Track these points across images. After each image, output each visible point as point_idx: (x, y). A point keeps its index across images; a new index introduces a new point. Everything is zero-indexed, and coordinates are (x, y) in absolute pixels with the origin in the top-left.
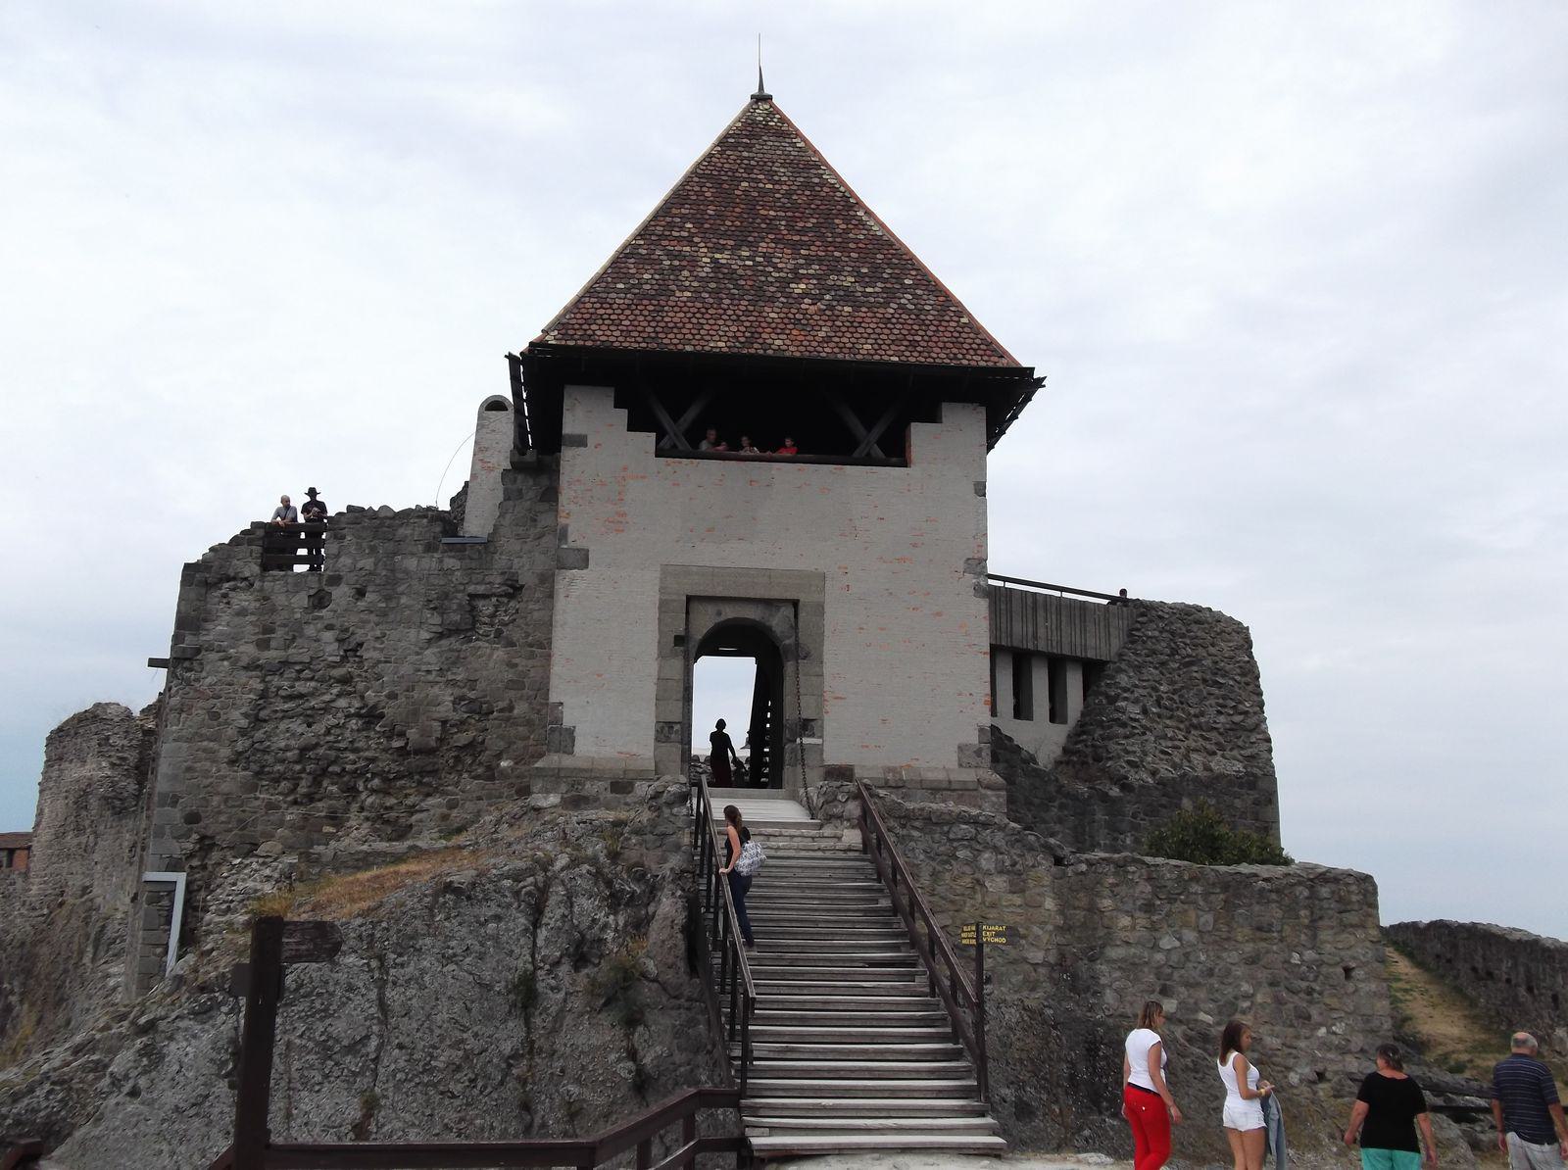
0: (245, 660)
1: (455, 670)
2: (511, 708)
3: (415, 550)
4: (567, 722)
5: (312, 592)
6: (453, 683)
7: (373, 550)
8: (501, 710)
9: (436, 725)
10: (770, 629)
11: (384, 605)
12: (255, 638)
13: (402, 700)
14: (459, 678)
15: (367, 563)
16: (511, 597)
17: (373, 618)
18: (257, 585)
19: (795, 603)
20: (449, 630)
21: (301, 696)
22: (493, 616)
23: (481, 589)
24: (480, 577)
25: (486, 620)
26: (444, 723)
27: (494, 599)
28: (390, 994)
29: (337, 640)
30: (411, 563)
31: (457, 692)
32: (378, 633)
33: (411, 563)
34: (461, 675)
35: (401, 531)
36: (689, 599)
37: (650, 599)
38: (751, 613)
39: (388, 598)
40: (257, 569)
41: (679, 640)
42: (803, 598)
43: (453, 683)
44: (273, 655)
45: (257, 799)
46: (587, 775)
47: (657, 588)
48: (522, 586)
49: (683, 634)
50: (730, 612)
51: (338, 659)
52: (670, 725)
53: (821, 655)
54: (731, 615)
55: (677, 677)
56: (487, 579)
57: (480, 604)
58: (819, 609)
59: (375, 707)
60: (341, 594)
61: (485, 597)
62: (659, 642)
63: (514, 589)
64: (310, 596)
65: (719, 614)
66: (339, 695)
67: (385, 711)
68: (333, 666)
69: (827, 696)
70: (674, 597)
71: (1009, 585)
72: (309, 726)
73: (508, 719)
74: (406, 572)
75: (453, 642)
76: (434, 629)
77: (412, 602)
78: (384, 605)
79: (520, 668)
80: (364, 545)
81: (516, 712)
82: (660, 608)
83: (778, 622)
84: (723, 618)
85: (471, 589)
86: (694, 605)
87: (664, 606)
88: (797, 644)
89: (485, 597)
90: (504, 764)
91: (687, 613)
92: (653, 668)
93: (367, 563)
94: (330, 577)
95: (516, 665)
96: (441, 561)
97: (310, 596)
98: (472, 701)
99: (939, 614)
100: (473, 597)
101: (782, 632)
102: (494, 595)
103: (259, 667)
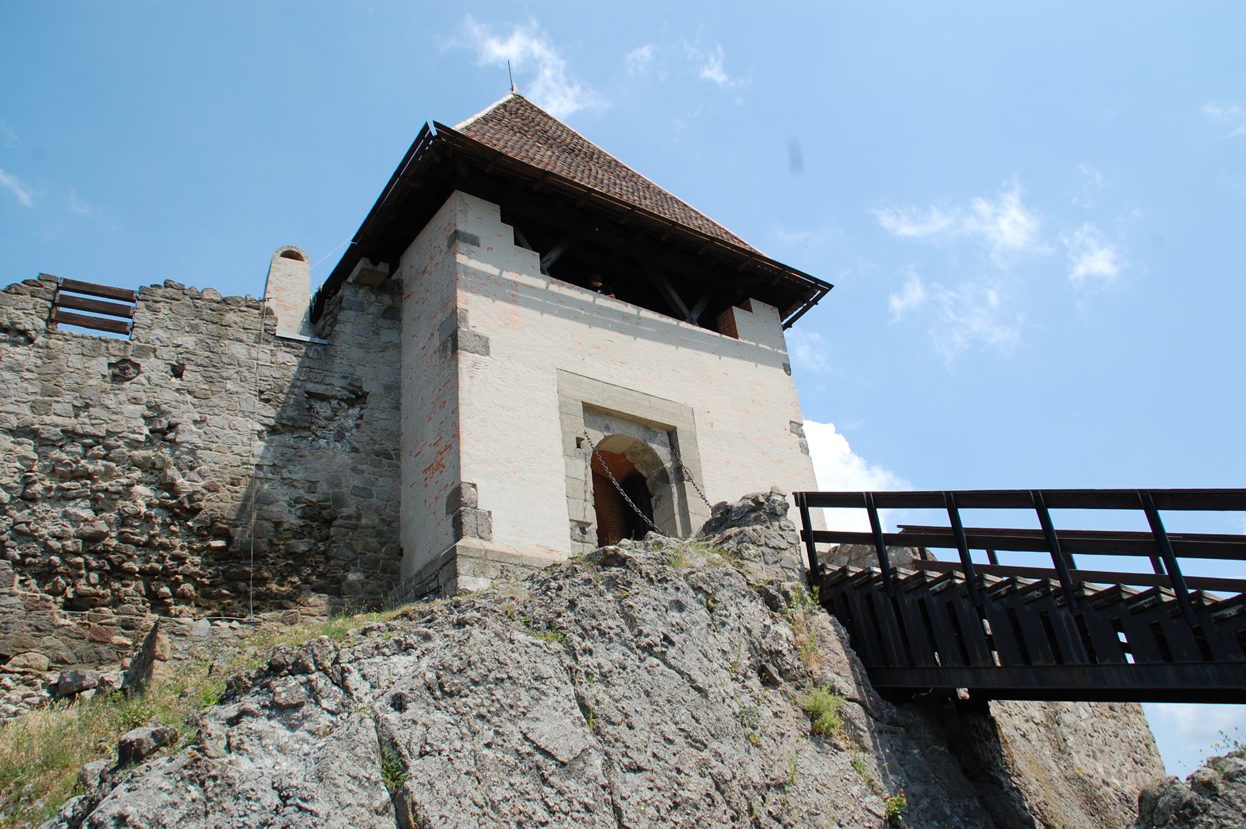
0: (14, 422)
1: (292, 468)
2: (359, 517)
3: (244, 337)
4: (483, 506)
5: (113, 360)
6: (291, 483)
7: (194, 329)
8: (349, 517)
9: (268, 525)
11: (206, 387)
12: (32, 398)
13: (224, 493)
14: (295, 477)
15: (189, 341)
16: (351, 403)
17: (189, 398)
18: (40, 340)
20: (284, 425)
21: (89, 476)
22: (331, 419)
23: (320, 389)
24: (320, 378)
25: (323, 423)
26: (278, 524)
27: (334, 402)
28: (593, 691)
29: (145, 417)
30: (239, 351)
31: (296, 493)
32: (197, 417)
33: (239, 351)
34: (299, 474)
35: (231, 317)
37: (551, 400)
39: (209, 380)
40: (43, 324)
43: (291, 483)
44: (57, 419)
45: (11, 595)
46: (516, 562)
48: (365, 395)
50: (618, 429)
51: (142, 438)
54: (618, 432)
56: (327, 380)
57: (317, 405)
59: (190, 497)
60: (153, 367)
61: (323, 398)
63: (357, 397)
64: (110, 365)
66: (139, 482)
67: (202, 504)
68: (134, 445)
71: (677, 517)
72: (97, 512)
73: (355, 528)
74: (232, 357)
75: (288, 438)
76: (266, 421)
77: (240, 390)
78: (206, 387)
79: (366, 475)
80: (183, 322)
81: (363, 521)
82: (560, 407)
85: (310, 387)
88: (679, 469)
89: (323, 398)
90: (352, 577)
92: (560, 463)
93: (189, 341)
94: (140, 348)
95: (363, 472)
96: (273, 355)
97: (110, 365)
98: (310, 505)
99: (780, 461)
100: (311, 395)
102: (335, 397)
103: (33, 434)
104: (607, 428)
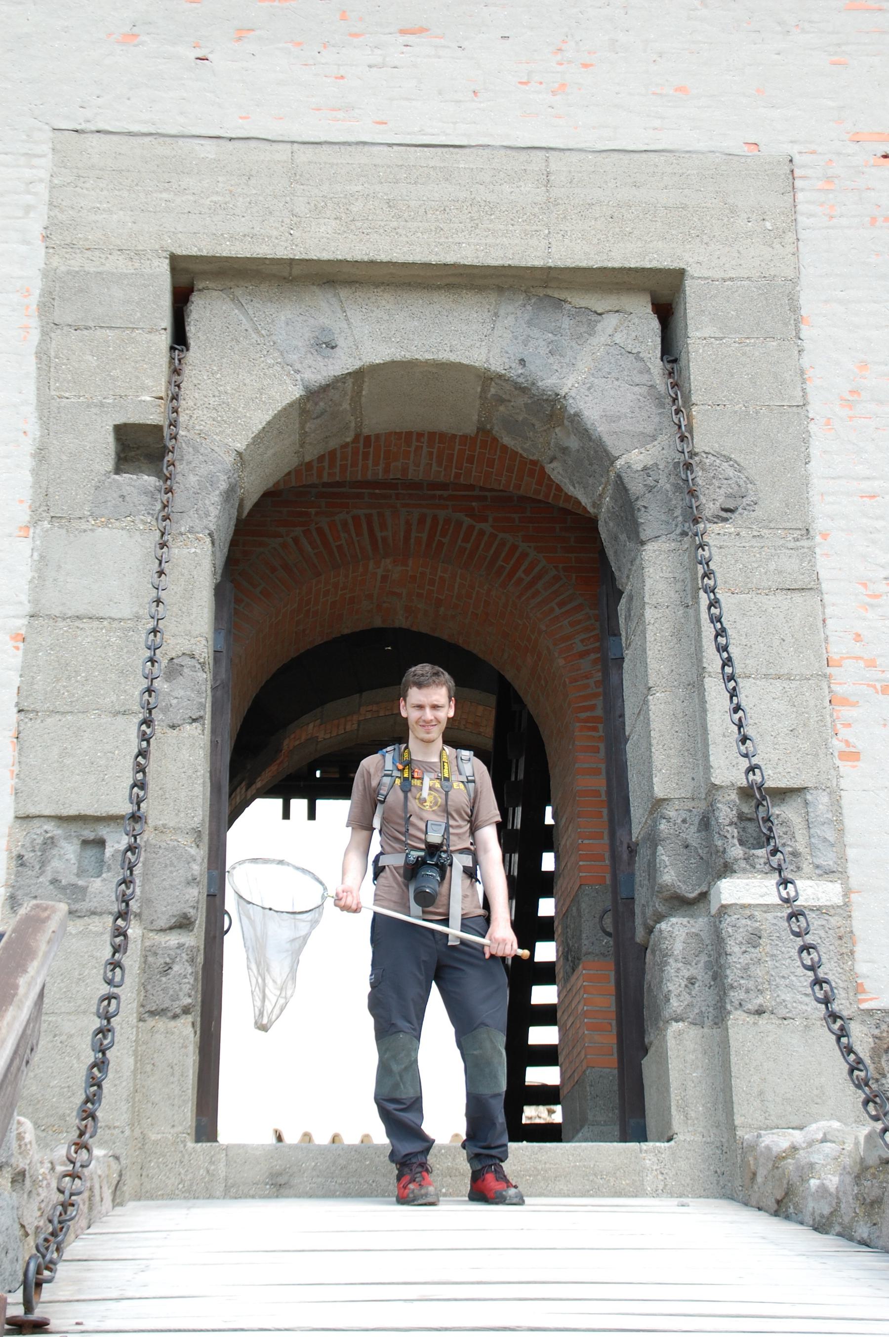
10: (551, 410)
19: (664, 296)
36: (186, 282)
38: (474, 340)
41: (142, 448)
42: (702, 263)
47: (36, 226)
49: (154, 416)
50: (376, 336)
52: (88, 829)
53: (799, 496)
55: (125, 610)
58: (780, 307)
62: (41, 454)
65: (326, 345)
69: (846, 680)
70: (118, 264)
82: (46, 307)
83: (597, 378)
84: (342, 363)
86: (207, 313)
87: (64, 307)
91: (180, 339)
101: (612, 419)
104: (326, 345)
